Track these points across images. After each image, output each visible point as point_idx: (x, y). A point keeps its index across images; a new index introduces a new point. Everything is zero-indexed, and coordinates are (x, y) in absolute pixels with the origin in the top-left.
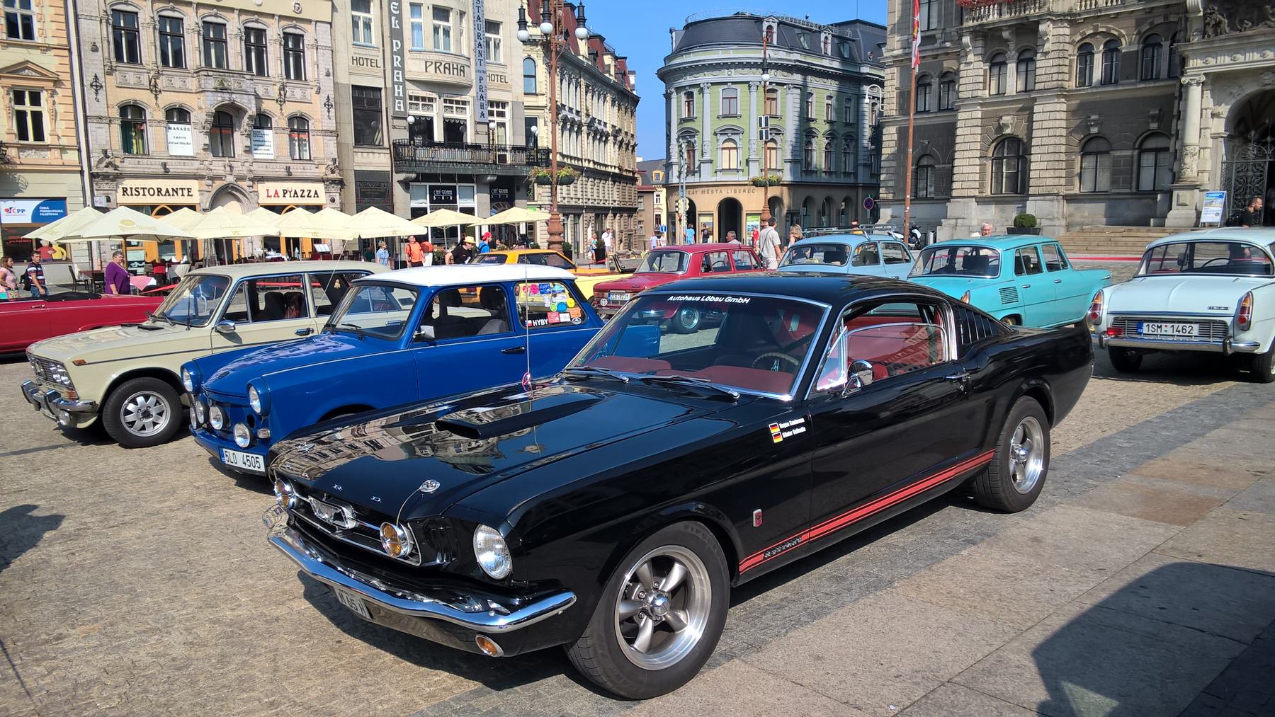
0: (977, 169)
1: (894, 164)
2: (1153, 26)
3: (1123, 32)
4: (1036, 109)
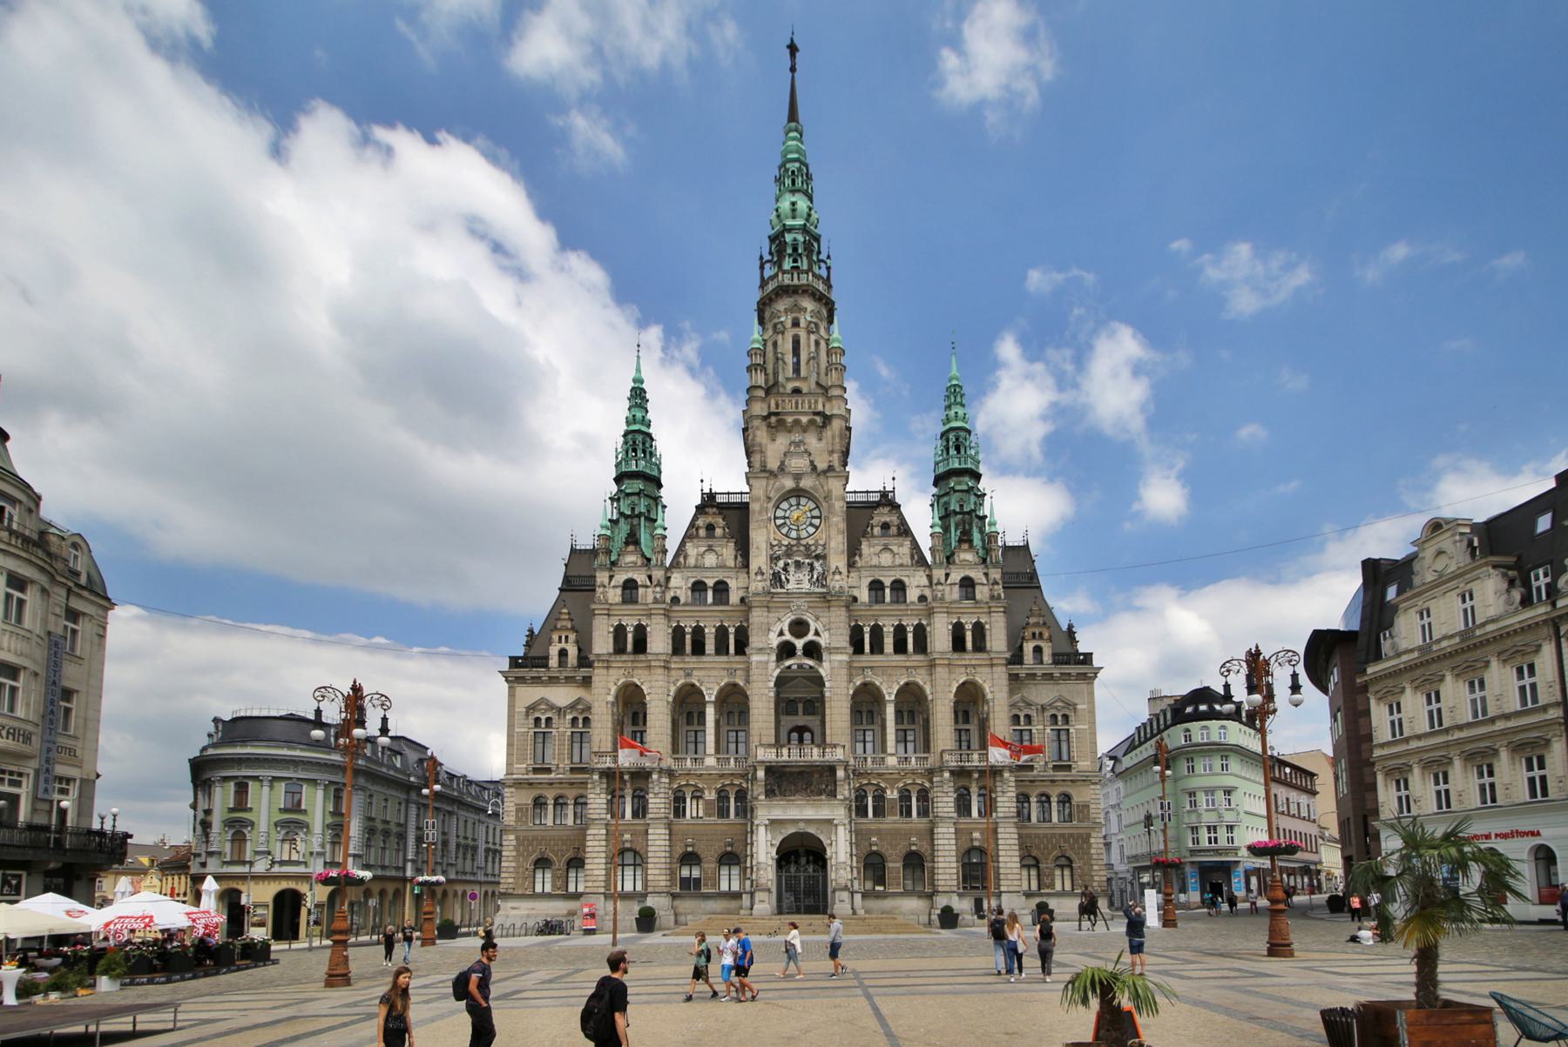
0: (604, 872)
1: (513, 864)
2: (724, 786)
4: (650, 831)
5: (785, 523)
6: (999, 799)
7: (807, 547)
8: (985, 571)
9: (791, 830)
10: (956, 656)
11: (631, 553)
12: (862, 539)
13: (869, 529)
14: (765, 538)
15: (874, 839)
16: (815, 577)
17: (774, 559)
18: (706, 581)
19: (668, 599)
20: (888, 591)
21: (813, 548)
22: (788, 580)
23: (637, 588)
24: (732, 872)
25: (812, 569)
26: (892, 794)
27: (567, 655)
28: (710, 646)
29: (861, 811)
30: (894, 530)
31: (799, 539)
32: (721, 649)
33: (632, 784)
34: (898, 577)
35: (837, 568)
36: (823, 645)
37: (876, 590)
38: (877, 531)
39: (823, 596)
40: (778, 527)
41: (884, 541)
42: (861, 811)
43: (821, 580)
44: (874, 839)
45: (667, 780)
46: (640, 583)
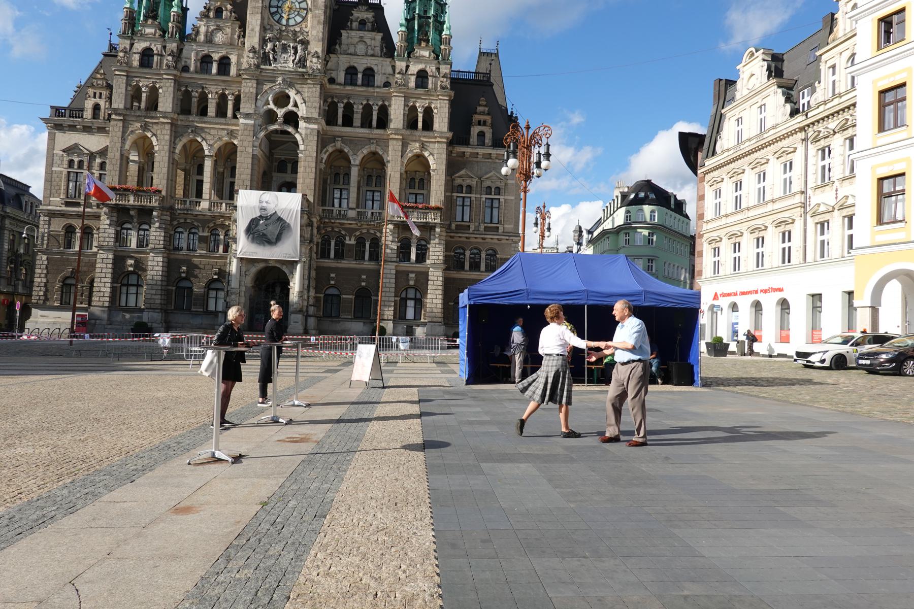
3: (200, 225)
5: (277, 11)
6: (431, 249)
7: (295, 33)
8: (438, 66)
9: (262, 265)
10: (408, 132)
11: (150, 26)
12: (342, 31)
13: (349, 24)
14: (259, 22)
15: (333, 275)
16: (297, 58)
17: (263, 41)
18: (213, 55)
19: (180, 66)
20: (360, 76)
21: (299, 34)
22: (275, 60)
23: (153, 56)
24: (219, 296)
25: (296, 53)
26: (350, 241)
27: (99, 109)
28: (212, 110)
29: (324, 254)
30: (369, 25)
31: (287, 25)
32: (221, 112)
33: (138, 220)
34: (369, 65)
35: (316, 52)
36: (300, 114)
37: (352, 74)
38: (355, 25)
39: (303, 74)
40: (272, 14)
41: (361, 33)
42: (324, 254)
43: (302, 62)
44: (333, 275)
45: (168, 218)
46: (155, 52)
